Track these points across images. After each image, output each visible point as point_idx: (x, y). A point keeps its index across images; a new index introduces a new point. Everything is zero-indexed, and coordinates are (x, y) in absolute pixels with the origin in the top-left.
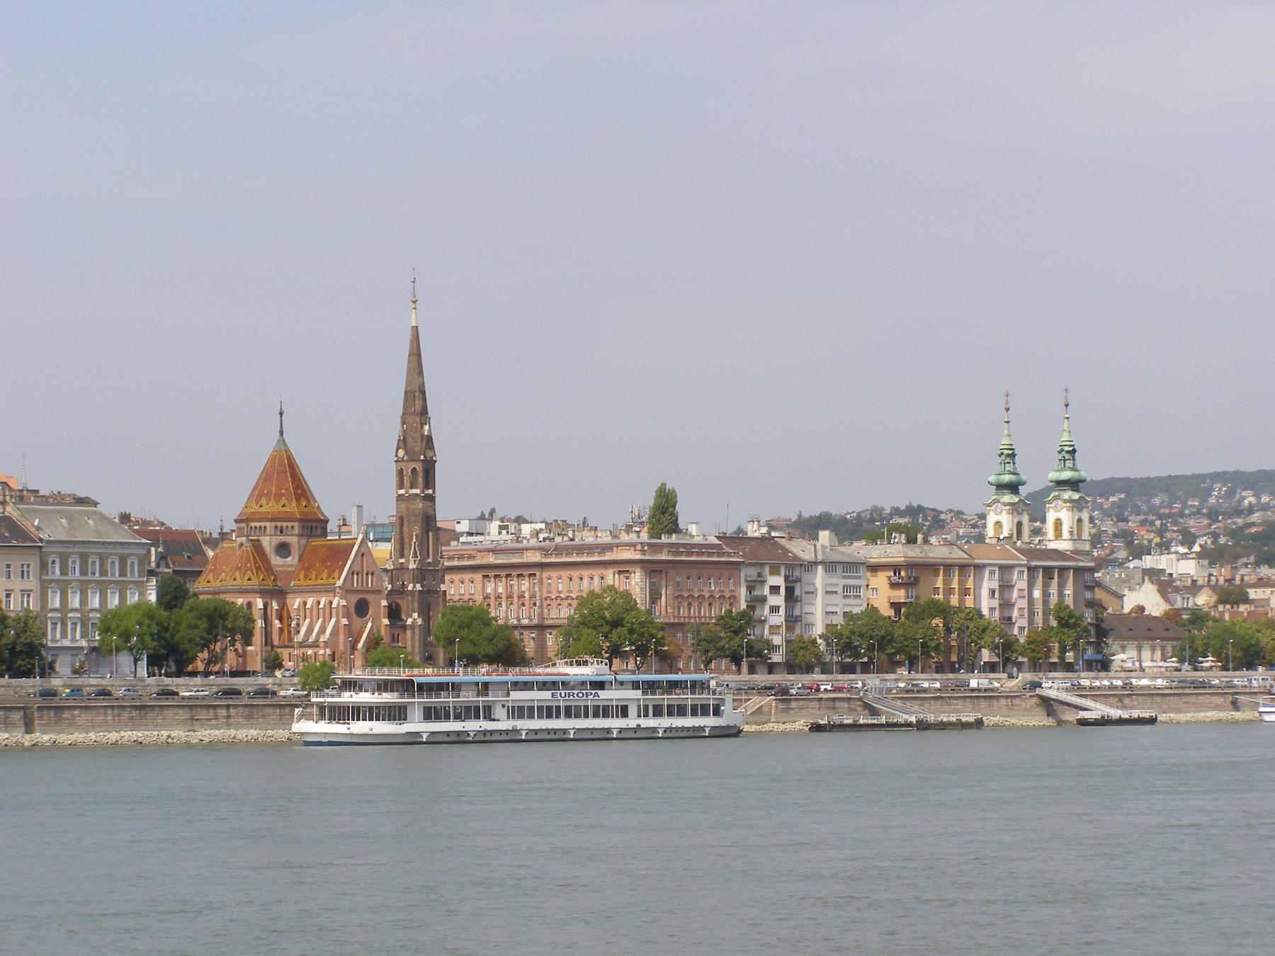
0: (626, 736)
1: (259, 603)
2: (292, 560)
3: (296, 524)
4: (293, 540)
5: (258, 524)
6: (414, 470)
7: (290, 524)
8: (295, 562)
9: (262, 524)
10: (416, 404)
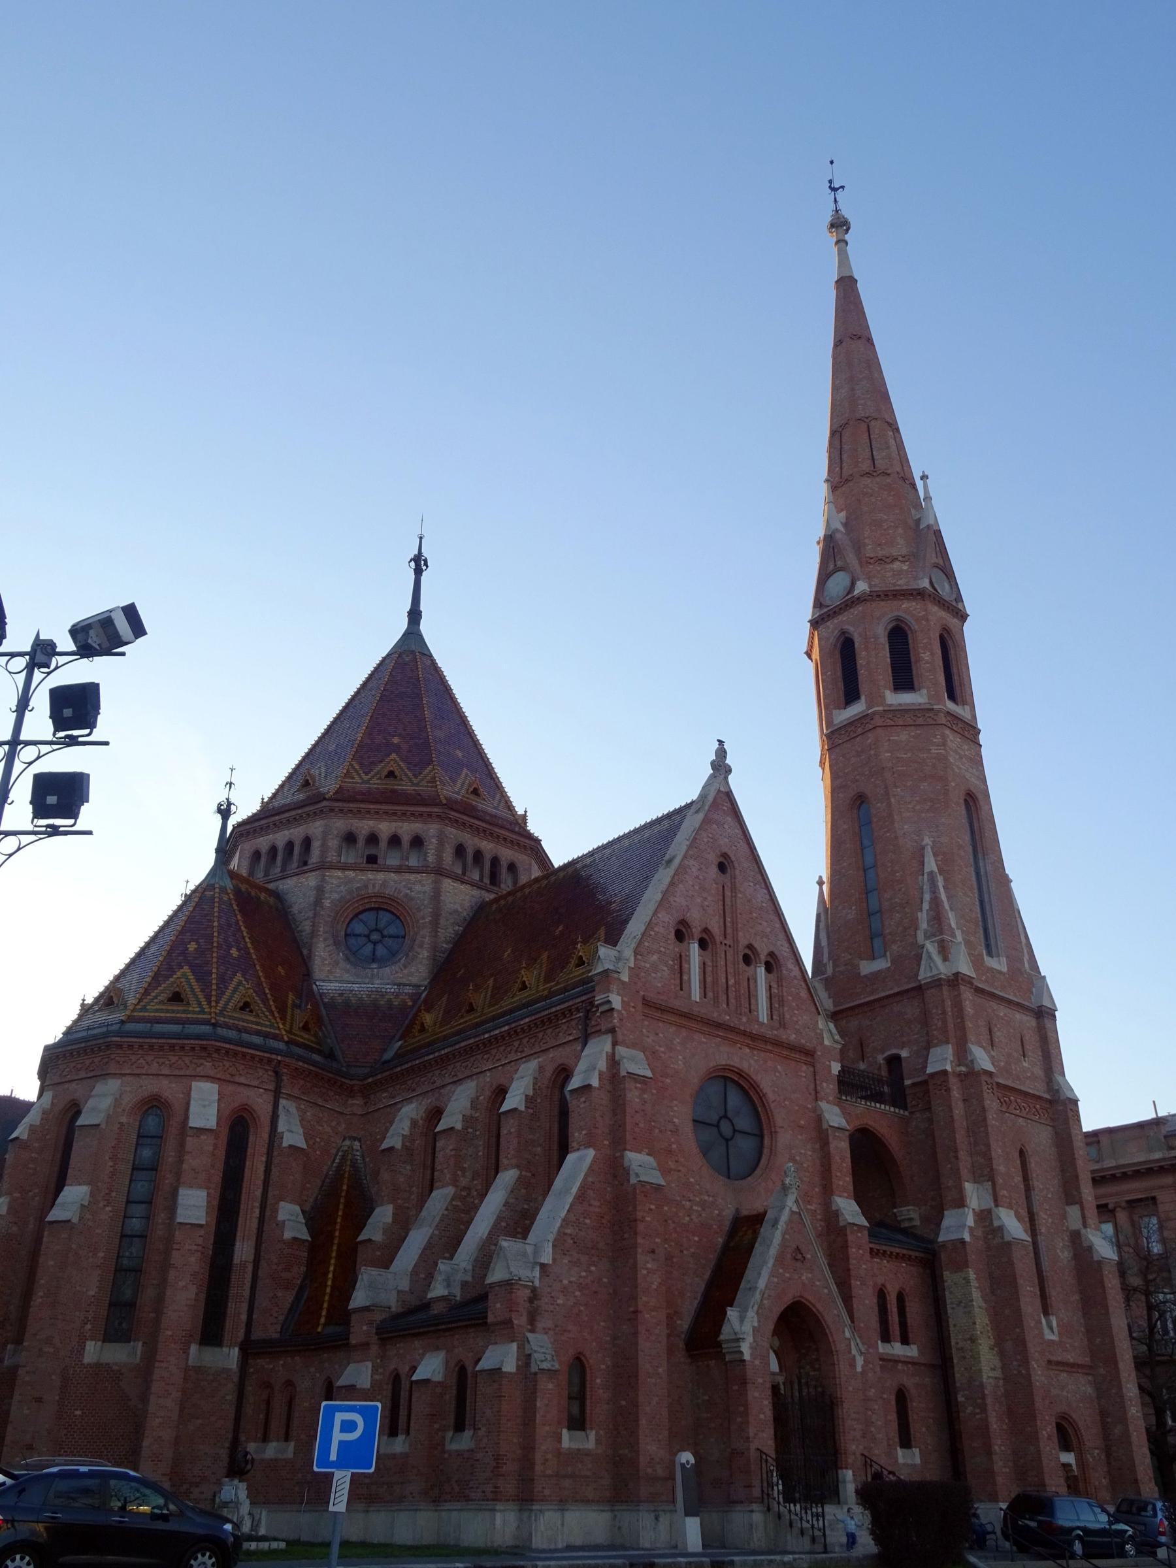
5: (280, 838)
7: (407, 830)
9: (296, 833)
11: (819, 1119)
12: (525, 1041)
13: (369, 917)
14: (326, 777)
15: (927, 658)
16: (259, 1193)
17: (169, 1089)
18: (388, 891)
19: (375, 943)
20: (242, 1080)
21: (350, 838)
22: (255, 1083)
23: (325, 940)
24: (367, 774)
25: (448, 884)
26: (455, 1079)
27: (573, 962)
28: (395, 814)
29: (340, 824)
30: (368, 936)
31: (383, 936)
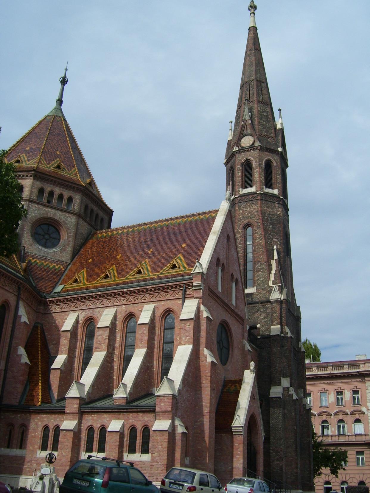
2: (59, 254)
3: (77, 198)
6: (268, 164)
7: (67, 194)
8: (66, 256)
11: (244, 346)
12: (147, 295)
13: (45, 227)
14: (28, 161)
15: (277, 178)
16: (8, 340)
18: (57, 218)
19: (47, 240)
20: (6, 288)
21: (41, 191)
22: (11, 291)
23: (27, 233)
24: (48, 164)
26: (103, 306)
27: (170, 265)
28: (63, 185)
30: (44, 236)
31: (50, 237)
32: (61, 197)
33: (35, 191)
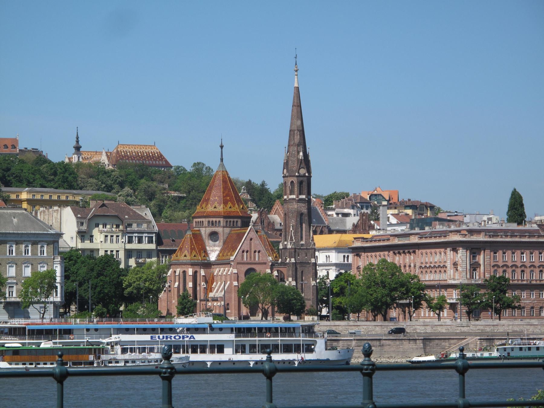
0: (219, 369)
1: (190, 271)
4: (219, 230)
6: (292, 182)
7: (218, 220)
10: (77, 138)
17: (186, 269)
21: (209, 222)
25: (225, 229)
29: (207, 219)
32: (216, 221)
33: (207, 223)
